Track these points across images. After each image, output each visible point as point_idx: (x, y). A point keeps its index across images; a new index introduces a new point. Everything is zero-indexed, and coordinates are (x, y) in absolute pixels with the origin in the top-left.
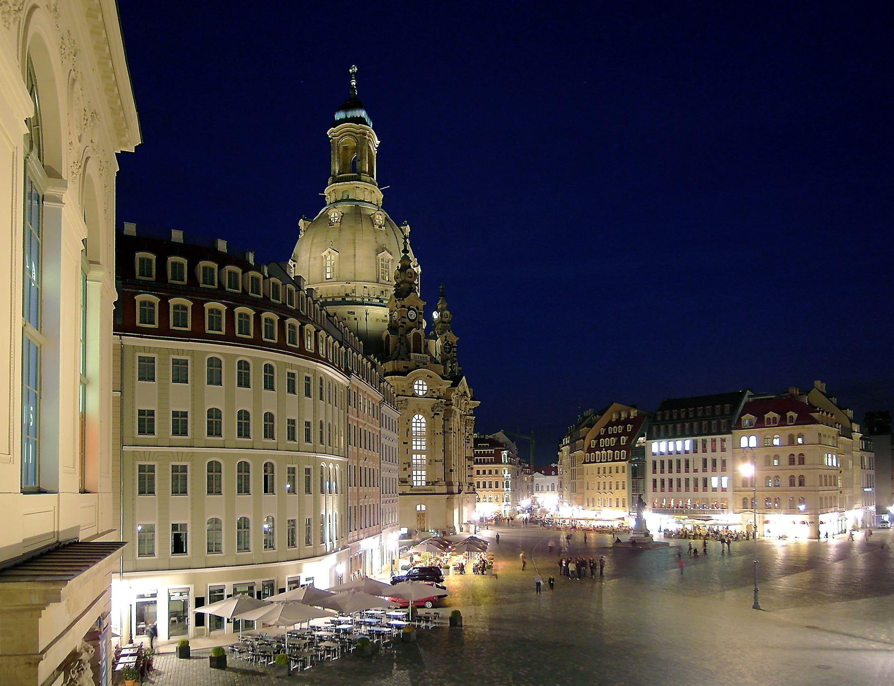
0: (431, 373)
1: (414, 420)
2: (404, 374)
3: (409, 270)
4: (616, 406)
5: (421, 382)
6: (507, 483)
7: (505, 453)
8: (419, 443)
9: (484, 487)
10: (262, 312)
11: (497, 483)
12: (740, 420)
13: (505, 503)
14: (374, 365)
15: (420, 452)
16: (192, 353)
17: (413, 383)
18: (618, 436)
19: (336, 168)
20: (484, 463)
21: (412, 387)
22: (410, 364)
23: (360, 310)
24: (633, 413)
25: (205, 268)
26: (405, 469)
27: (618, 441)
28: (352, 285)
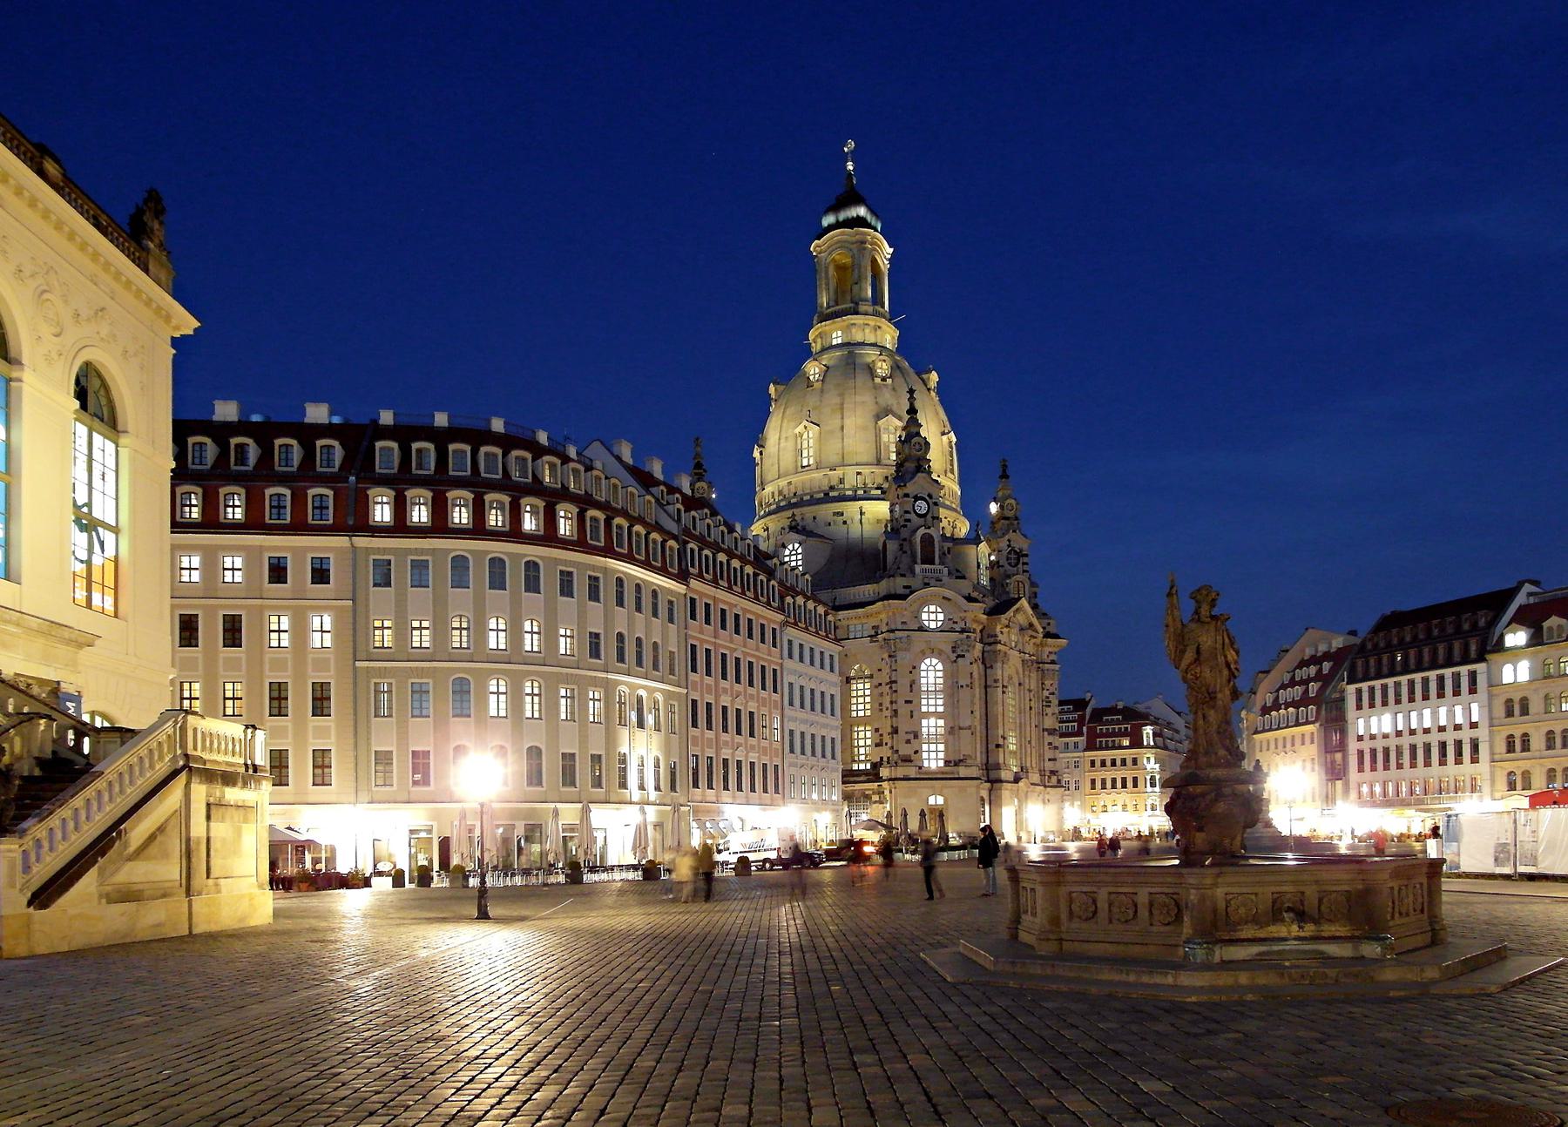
0: (948, 593)
1: (923, 667)
2: (903, 597)
3: (916, 439)
4: (1311, 634)
5: (932, 608)
6: (1152, 778)
8: (932, 702)
9: (1124, 786)
11: (1135, 780)
12: (1502, 637)
13: (1150, 812)
16: (433, 551)
21: (917, 617)
22: (914, 582)
24: (1338, 642)
26: (908, 742)
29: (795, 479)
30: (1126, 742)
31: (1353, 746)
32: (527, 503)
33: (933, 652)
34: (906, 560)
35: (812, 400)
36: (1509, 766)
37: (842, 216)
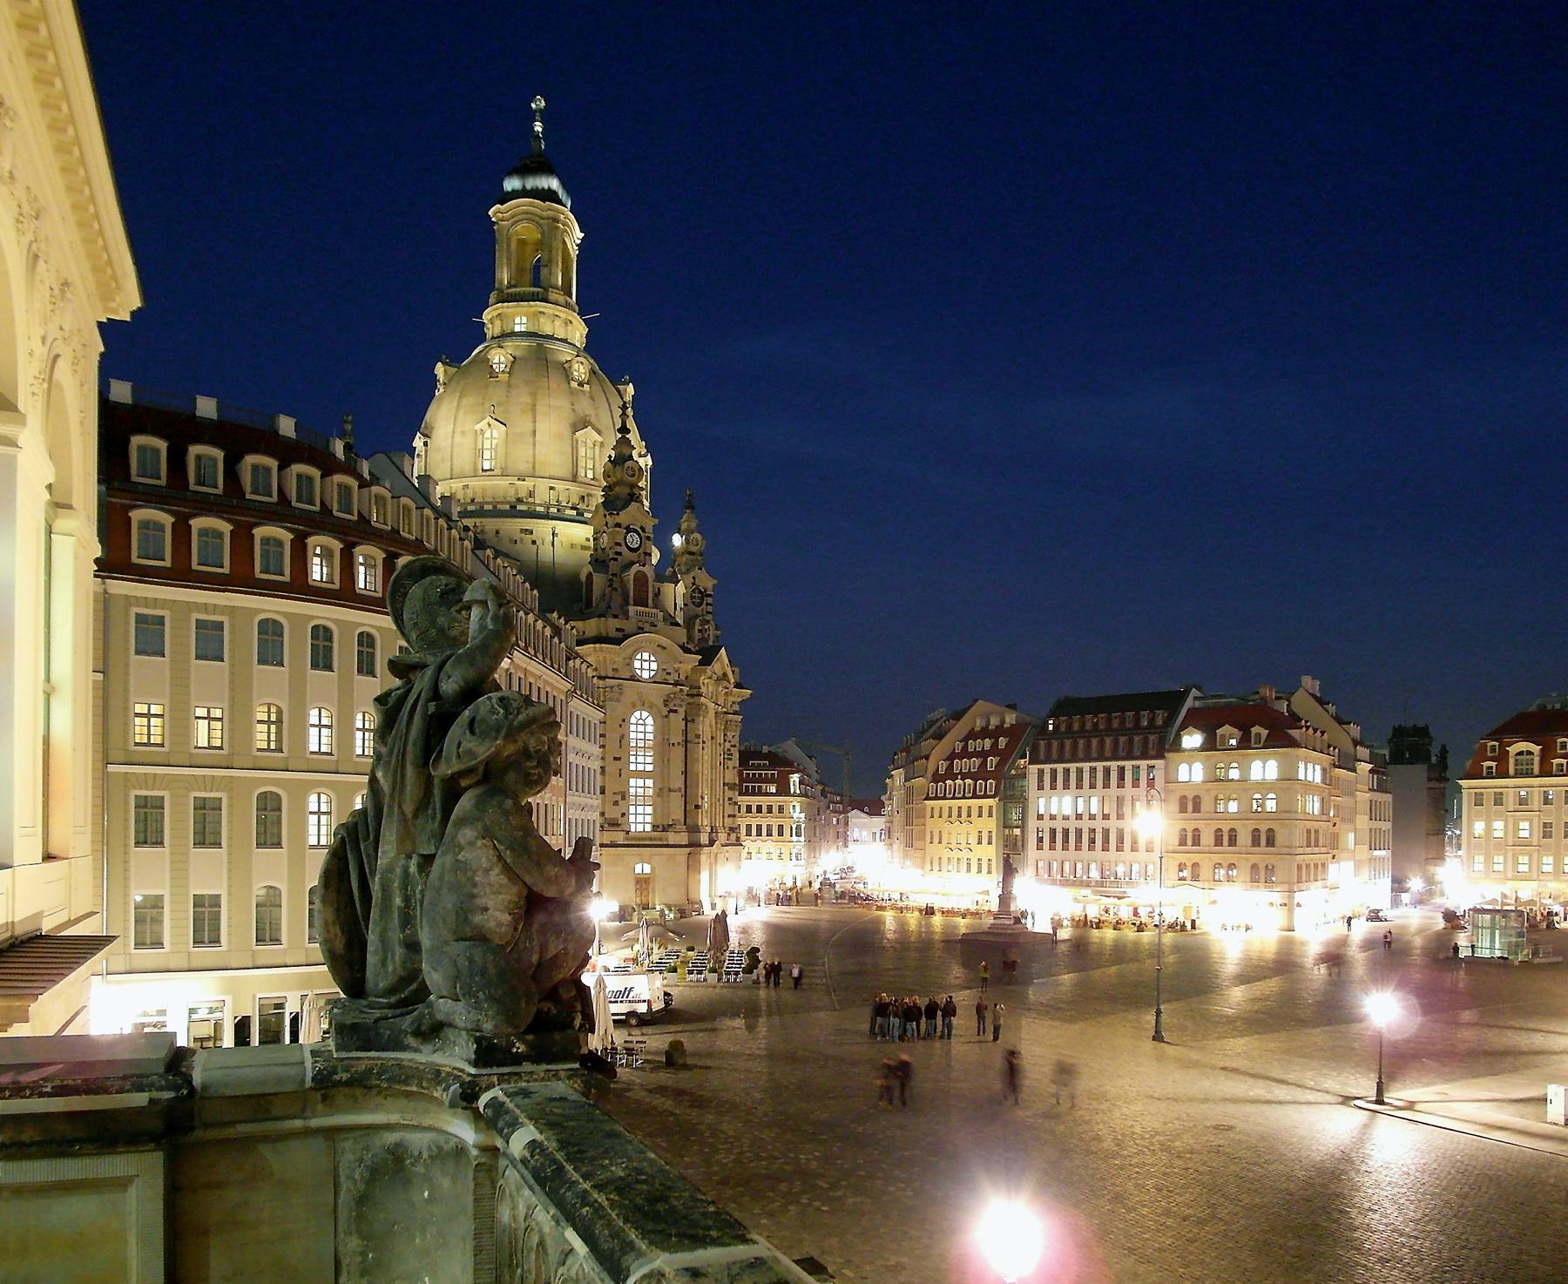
1: (633, 720)
3: (629, 463)
5: (646, 656)
6: (798, 828)
7: (795, 778)
9: (759, 834)
10: (354, 545)
11: (781, 827)
14: (557, 631)
15: (643, 775)
16: (232, 611)
17: (632, 658)
18: (983, 755)
19: (504, 276)
20: (760, 794)
21: (630, 665)
22: (629, 626)
23: (542, 528)
25: (255, 468)
26: (616, 803)
27: (984, 764)
28: (529, 483)
29: (472, 483)
30: (773, 789)
31: (1032, 824)
32: (316, 542)
33: (643, 704)
34: (617, 599)
35: (498, 394)
36: (1182, 858)
37: (531, 183)
